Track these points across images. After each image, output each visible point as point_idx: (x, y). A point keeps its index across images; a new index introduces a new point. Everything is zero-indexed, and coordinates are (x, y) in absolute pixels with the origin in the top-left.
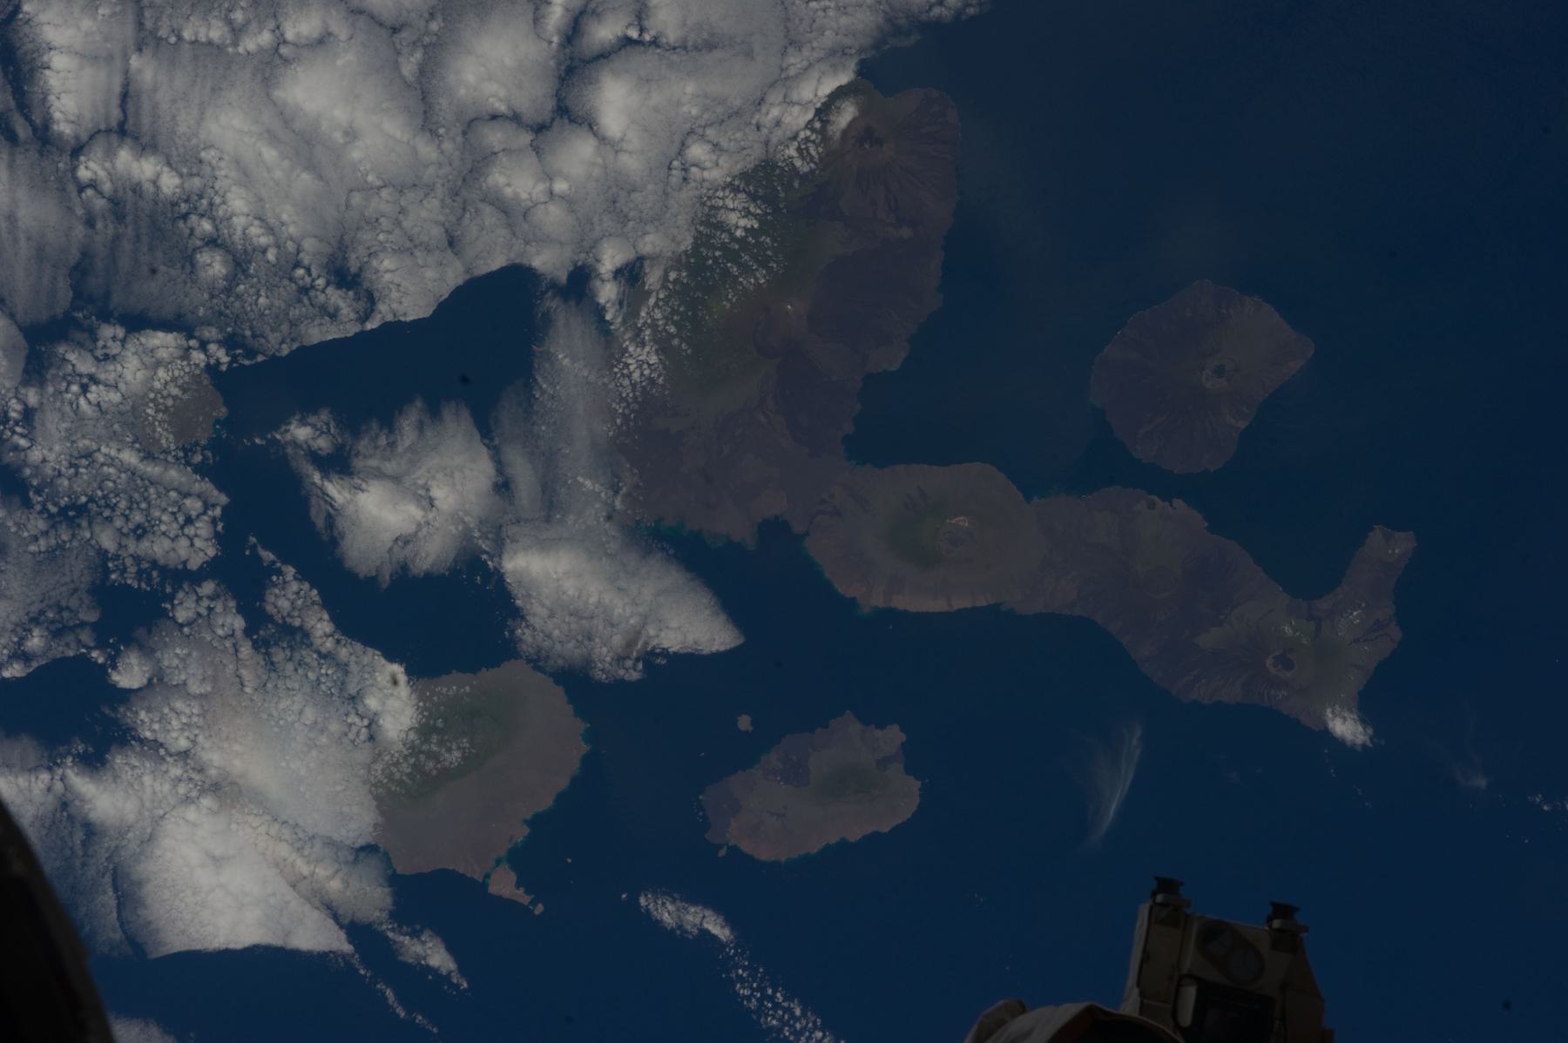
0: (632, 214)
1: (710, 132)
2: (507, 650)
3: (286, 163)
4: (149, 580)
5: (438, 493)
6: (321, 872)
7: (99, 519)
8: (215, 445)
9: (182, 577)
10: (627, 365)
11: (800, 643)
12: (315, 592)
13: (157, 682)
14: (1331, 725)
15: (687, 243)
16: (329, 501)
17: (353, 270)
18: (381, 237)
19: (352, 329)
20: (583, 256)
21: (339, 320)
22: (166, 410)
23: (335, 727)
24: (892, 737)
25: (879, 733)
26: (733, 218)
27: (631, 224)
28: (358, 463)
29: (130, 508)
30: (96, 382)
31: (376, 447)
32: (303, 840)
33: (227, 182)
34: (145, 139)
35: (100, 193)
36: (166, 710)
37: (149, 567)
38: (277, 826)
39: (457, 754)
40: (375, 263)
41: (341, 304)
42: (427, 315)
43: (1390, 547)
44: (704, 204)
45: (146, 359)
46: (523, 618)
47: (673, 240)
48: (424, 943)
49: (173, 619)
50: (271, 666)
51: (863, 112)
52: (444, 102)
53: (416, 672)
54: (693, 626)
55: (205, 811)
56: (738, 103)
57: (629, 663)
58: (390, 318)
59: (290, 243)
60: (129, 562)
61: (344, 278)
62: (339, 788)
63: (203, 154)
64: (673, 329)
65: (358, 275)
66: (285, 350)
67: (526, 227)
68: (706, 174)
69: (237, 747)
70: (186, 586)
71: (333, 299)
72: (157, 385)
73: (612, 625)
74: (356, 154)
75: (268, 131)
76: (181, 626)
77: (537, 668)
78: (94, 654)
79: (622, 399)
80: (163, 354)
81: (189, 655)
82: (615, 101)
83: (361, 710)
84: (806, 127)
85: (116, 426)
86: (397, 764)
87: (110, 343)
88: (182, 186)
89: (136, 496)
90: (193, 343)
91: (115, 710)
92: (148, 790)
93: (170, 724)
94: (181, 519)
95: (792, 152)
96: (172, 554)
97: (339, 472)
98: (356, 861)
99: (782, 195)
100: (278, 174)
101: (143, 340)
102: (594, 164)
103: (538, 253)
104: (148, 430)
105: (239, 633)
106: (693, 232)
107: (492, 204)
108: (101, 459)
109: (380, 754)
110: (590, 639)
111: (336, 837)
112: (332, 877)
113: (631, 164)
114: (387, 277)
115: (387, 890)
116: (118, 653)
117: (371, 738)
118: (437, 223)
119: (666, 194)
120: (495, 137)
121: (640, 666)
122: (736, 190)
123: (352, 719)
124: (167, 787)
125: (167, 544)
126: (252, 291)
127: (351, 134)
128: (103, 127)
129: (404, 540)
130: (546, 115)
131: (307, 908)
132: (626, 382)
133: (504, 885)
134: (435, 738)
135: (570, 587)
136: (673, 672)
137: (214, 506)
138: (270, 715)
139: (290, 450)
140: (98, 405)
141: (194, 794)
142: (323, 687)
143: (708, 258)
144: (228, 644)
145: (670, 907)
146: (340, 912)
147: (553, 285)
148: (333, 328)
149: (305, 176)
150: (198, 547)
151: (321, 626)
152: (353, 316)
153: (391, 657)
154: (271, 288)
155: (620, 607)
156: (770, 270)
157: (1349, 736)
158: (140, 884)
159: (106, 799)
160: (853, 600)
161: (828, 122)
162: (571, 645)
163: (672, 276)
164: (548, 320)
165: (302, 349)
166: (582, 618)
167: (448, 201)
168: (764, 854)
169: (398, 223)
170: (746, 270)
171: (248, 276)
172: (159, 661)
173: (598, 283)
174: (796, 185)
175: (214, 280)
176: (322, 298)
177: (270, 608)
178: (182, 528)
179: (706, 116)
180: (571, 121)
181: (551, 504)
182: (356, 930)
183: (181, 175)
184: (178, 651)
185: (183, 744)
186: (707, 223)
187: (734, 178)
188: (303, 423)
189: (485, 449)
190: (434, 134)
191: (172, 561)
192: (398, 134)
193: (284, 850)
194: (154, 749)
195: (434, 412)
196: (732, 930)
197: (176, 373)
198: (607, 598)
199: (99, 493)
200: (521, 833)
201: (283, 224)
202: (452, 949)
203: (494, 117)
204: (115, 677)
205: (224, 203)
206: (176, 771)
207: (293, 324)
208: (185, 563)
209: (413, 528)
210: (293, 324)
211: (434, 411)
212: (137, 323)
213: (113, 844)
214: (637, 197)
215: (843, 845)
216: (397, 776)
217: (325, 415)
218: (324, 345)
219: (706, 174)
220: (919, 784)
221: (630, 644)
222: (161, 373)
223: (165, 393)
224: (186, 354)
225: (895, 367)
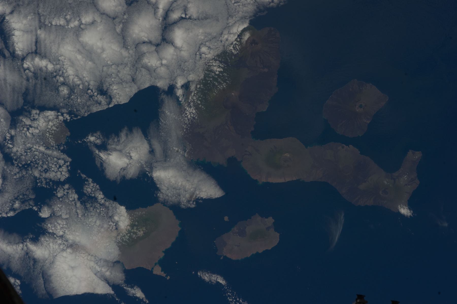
0: (186, 69)
1: (207, 43)
2: (155, 200)
3: (84, 59)
4: (49, 185)
5: (133, 154)
6: (104, 270)
7: (34, 168)
8: (67, 144)
9: (59, 183)
10: (186, 114)
11: (242, 195)
12: (98, 186)
13: (53, 215)
14: (400, 210)
15: (202, 77)
16: (101, 159)
17: (105, 90)
18: (113, 79)
19: (105, 107)
20: (172, 82)
23: (105, 226)
24: (270, 221)
25: (266, 220)
26: (215, 68)
27: (185, 72)
28: (109, 147)
29: (43, 164)
30: (32, 127)
31: (114, 142)
32: (98, 261)
33: (67, 66)
34: (43, 54)
35: (30, 71)
36: (56, 224)
38: (90, 256)
40: (111, 87)
41: (102, 100)
42: (127, 102)
43: (414, 156)
44: (206, 65)
46: (160, 190)
47: (198, 76)
49: (57, 196)
50: (86, 209)
51: (252, 35)
52: (129, 39)
53: (128, 208)
54: (210, 190)
55: (68, 253)
56: (215, 34)
57: (191, 202)
58: (116, 103)
60: (43, 180)
61: (103, 92)
62: (108, 244)
63: (60, 58)
64: (199, 102)
65: (106, 91)
67: (155, 74)
68: (207, 56)
69: (77, 234)
70: (60, 186)
71: (99, 99)
72: (49, 127)
73: (186, 191)
74: (104, 56)
75: (79, 50)
76: (59, 198)
77: (164, 205)
78: (34, 208)
79: (185, 124)
80: (51, 117)
81: (62, 207)
82: (179, 36)
83: (113, 220)
84: (235, 40)
86: (124, 236)
87: (35, 115)
88: (54, 68)
89: (44, 160)
90: (59, 114)
91: (41, 224)
92: (52, 248)
93: (57, 227)
94: (58, 166)
95: (231, 48)
96: (56, 177)
97: (103, 150)
98: (114, 266)
99: (229, 61)
100: (82, 63)
101: (45, 114)
102: (174, 55)
103: (159, 82)
104: (47, 140)
105: (76, 199)
106: (204, 73)
107: (145, 68)
108: (34, 150)
109: (119, 233)
110: (179, 196)
111: (108, 259)
112: (107, 271)
113: (185, 54)
114: (115, 91)
115: (123, 274)
116: (41, 207)
117: (117, 229)
118: (129, 74)
119: (195, 62)
120: (144, 48)
121: (195, 203)
122: (216, 60)
123: (111, 223)
124: (57, 247)
125: (54, 174)
126: (76, 98)
127: (103, 50)
128: (30, 52)
129: (124, 169)
130: (159, 41)
132: (186, 119)
133: (158, 271)
134: (135, 228)
135: (173, 181)
136: (204, 205)
137: (67, 162)
138: (86, 223)
139: (89, 144)
140: (32, 134)
141: (65, 248)
142: (102, 214)
144: (73, 203)
145: (207, 275)
147: (164, 91)
148: (100, 107)
149: (90, 63)
150: (63, 174)
151: (100, 196)
152: (105, 103)
153: (121, 205)
154: (81, 96)
155: (188, 186)
156: (227, 83)
157: (406, 214)
158: (50, 276)
159: (39, 251)
160: (256, 180)
161: (241, 38)
163: (198, 86)
164: (162, 101)
165: (91, 114)
166: (177, 190)
167: (132, 68)
168: (234, 258)
169: (117, 75)
170: (220, 83)
171: (74, 93)
172: (53, 209)
173: (177, 90)
174: (233, 58)
175: (65, 95)
176: (96, 98)
177: (85, 191)
178: (58, 169)
179: (206, 39)
180: (167, 42)
181: (166, 156)
183: (54, 65)
185: (61, 233)
186: (207, 70)
187: (215, 57)
188: (92, 136)
189: (146, 141)
190: (127, 48)
191: (56, 179)
192: (116, 49)
193: (92, 264)
194: (53, 235)
195: (131, 130)
197: (55, 123)
198: (184, 183)
199: (34, 160)
200: (162, 255)
201: (84, 77)
203: (144, 43)
204: (41, 214)
205: (66, 72)
206: (60, 242)
207: (88, 107)
208: (59, 179)
209: (126, 165)
210: (88, 107)
211: (130, 130)
212: (42, 109)
213: (42, 265)
214: (187, 64)
215: (257, 253)
216: (125, 240)
217: (99, 133)
218: (97, 112)
220: (279, 234)
221: (191, 197)
222: (50, 123)
223: (52, 129)
224: (57, 117)
225: (265, 111)
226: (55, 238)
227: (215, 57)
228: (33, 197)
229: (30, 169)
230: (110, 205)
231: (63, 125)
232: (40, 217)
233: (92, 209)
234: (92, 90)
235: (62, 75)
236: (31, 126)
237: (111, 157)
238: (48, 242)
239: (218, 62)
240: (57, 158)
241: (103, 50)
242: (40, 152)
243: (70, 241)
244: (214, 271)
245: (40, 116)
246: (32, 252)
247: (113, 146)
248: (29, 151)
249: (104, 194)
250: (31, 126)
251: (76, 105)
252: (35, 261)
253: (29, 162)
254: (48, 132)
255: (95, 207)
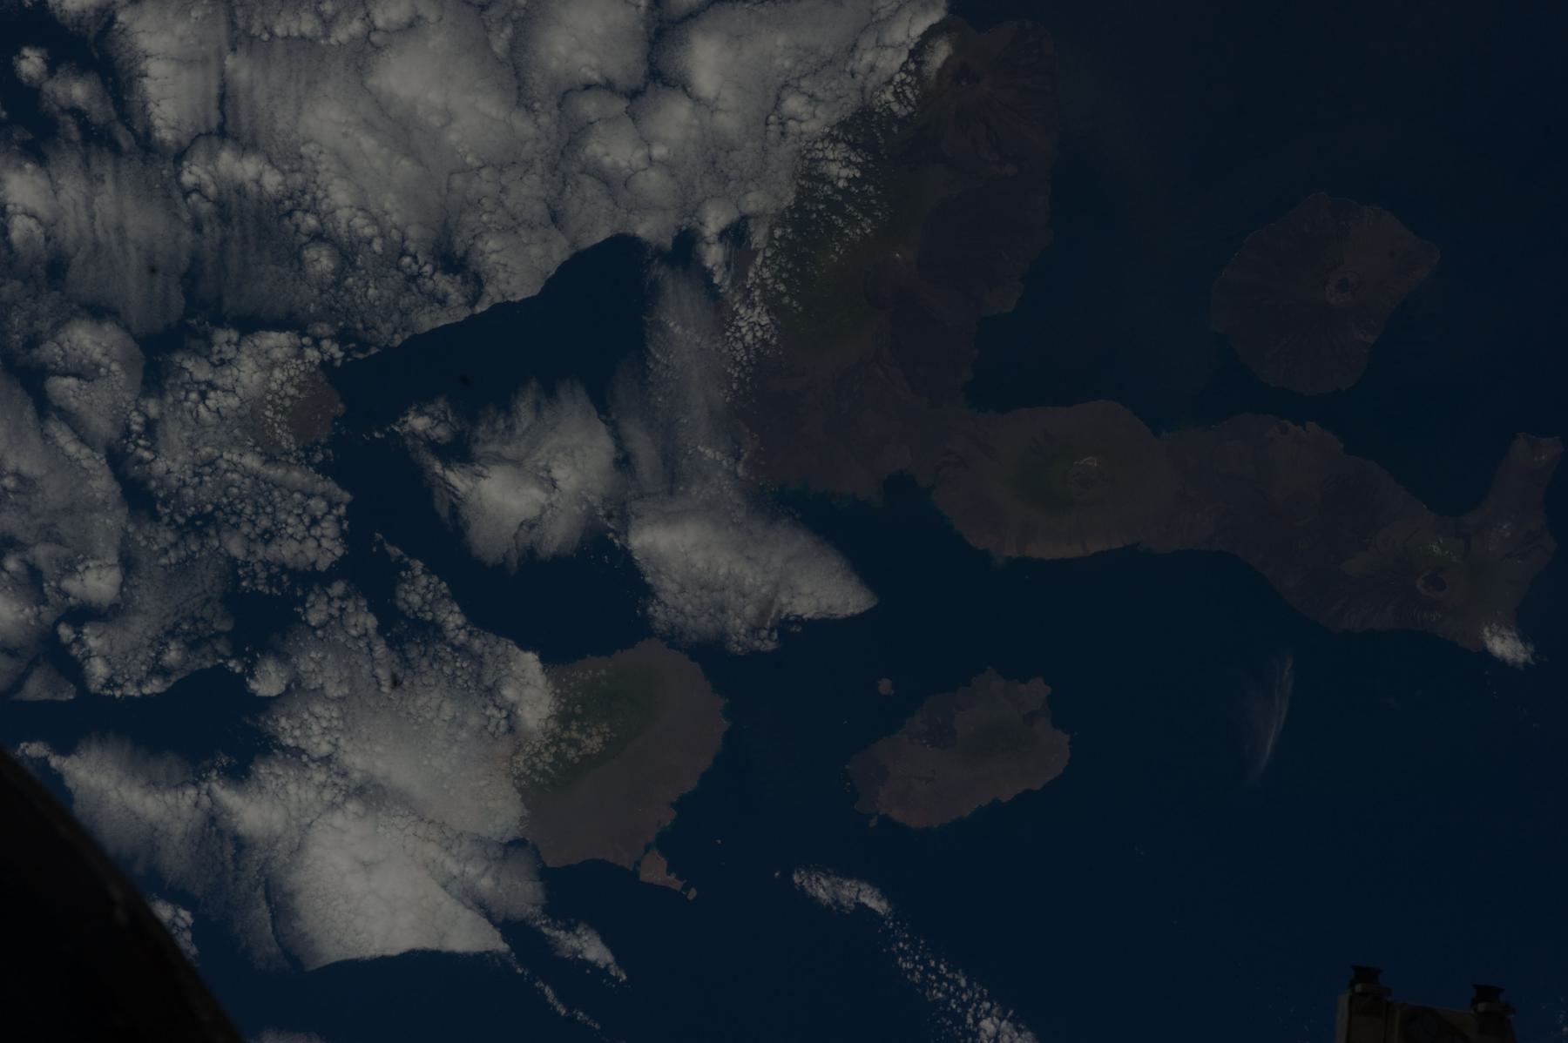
0: (732, 173)
2: (641, 629)
3: (385, 151)
4: (279, 585)
5: (560, 474)
9: (311, 579)
10: (739, 328)
12: (444, 585)
13: (295, 687)
15: (790, 198)
16: (453, 491)
17: (459, 253)
18: (485, 218)
19: (463, 314)
20: (686, 220)
21: (451, 306)
22: (284, 411)
23: (474, 721)
24: (1036, 691)
26: (834, 169)
27: (732, 183)
28: (478, 449)
29: (256, 513)
31: (495, 432)
36: (306, 716)
37: (280, 572)
38: (423, 826)
39: (598, 739)
40: (480, 245)
41: (450, 289)
44: (803, 157)
45: (261, 361)
46: (654, 595)
48: (579, 936)
49: (306, 622)
50: (406, 662)
53: (548, 660)
54: (825, 590)
57: (764, 633)
58: (498, 299)
59: (394, 232)
60: (258, 567)
61: (451, 261)
62: (482, 783)
63: (303, 149)
64: (782, 288)
65: (464, 259)
66: (398, 340)
68: (804, 127)
69: (379, 749)
70: (316, 588)
72: (274, 386)
73: (744, 596)
74: (453, 137)
75: (366, 121)
76: (314, 629)
78: (231, 664)
80: (278, 354)
83: (498, 702)
85: (236, 431)
86: (538, 754)
87: (225, 348)
88: (284, 183)
89: (261, 500)
90: (306, 340)
92: (294, 799)
93: (311, 728)
94: (307, 520)
95: (888, 96)
101: (257, 341)
105: (372, 632)
107: (592, 175)
108: (224, 466)
110: (723, 611)
112: (483, 875)
113: (728, 123)
114: (494, 257)
115: (539, 884)
116: (255, 660)
117: (511, 729)
120: (590, 107)
121: (775, 635)
122: (835, 140)
124: (312, 795)
125: (294, 546)
126: (360, 283)
127: (449, 117)
128: (203, 130)
129: (529, 525)
131: (460, 908)
132: (739, 346)
133: (655, 871)
134: (574, 725)
135: (699, 560)
136: (807, 639)
137: (338, 504)
139: (409, 442)
140: (218, 411)
141: (339, 799)
142: (460, 681)
143: (812, 212)
144: (362, 644)
145: (825, 883)
146: (494, 910)
147: (659, 252)
150: (325, 547)
151: (453, 619)
152: (462, 300)
153: (525, 646)
155: (751, 577)
158: (291, 895)
159: (253, 811)
162: (704, 619)
163: (778, 233)
165: (414, 337)
169: (500, 203)
171: (355, 269)
172: (295, 667)
173: (704, 247)
174: (895, 130)
177: (400, 604)
178: (308, 529)
181: (673, 477)
182: (509, 928)
183: (283, 173)
184: (313, 655)
185: (325, 748)
186: (808, 177)
187: (832, 128)
189: (602, 426)
190: (529, 109)
193: (432, 851)
196: (889, 903)
197: (292, 373)
199: (225, 500)
200: (668, 817)
201: (386, 213)
202: (607, 942)
204: (254, 686)
206: (320, 777)
207: (403, 313)
208: (314, 564)
209: (536, 512)
210: (403, 313)
212: (250, 325)
216: (540, 766)
219: (804, 127)
220: (1067, 737)
221: (763, 615)
224: (300, 352)
226: (306, 765)
227: (832, 128)
228: (225, 626)
229: (212, 532)
230: (487, 649)
231: (321, 380)
232: (253, 695)
233: (425, 662)
234: (415, 258)
235: (311, 209)
236: (211, 386)
237: (484, 483)
238: (282, 780)
239: (842, 146)
240: (304, 494)
241: (449, 117)
242: (247, 473)
243: (356, 776)
244: (847, 871)
245: (243, 349)
246: (230, 814)
247: (493, 448)
248: (208, 470)
249: (465, 610)
250: (211, 386)
251: (362, 308)
252: (240, 844)
253: (209, 508)
254: (271, 402)
255: (436, 658)
